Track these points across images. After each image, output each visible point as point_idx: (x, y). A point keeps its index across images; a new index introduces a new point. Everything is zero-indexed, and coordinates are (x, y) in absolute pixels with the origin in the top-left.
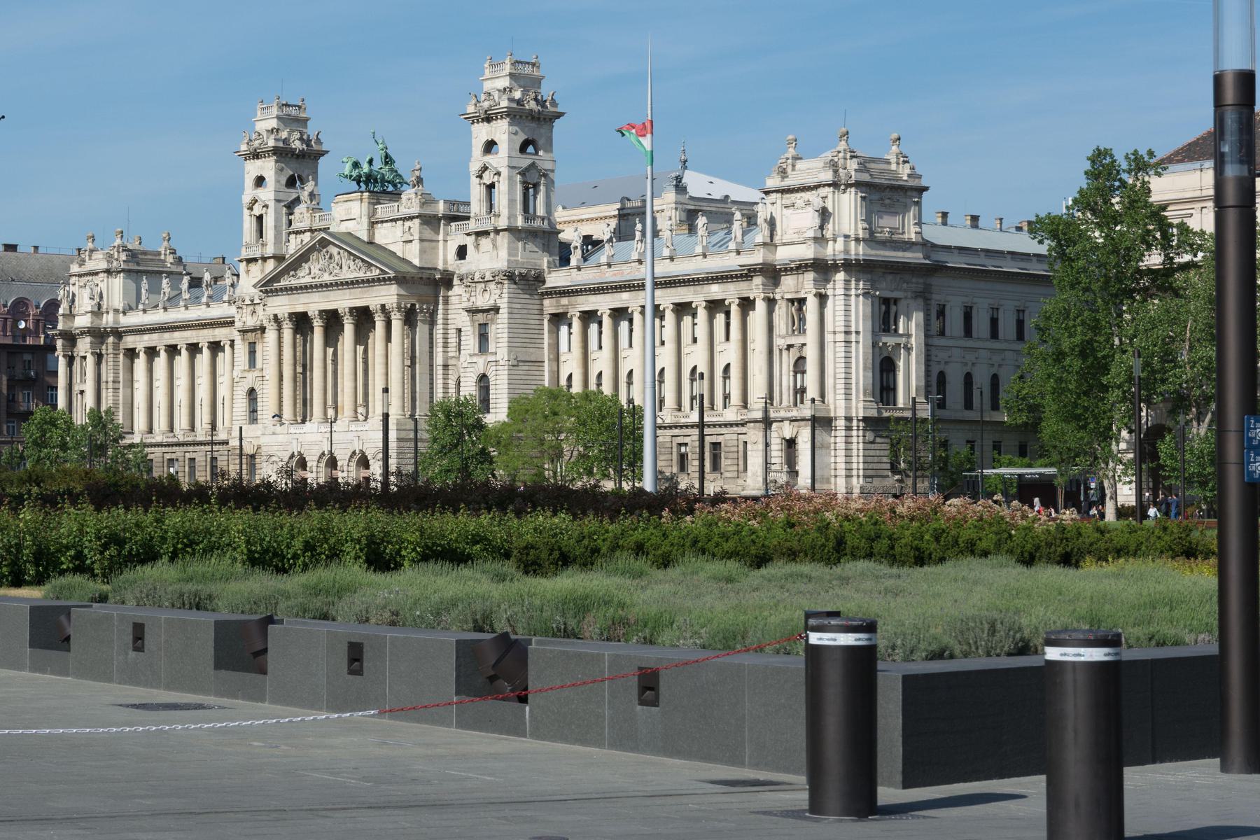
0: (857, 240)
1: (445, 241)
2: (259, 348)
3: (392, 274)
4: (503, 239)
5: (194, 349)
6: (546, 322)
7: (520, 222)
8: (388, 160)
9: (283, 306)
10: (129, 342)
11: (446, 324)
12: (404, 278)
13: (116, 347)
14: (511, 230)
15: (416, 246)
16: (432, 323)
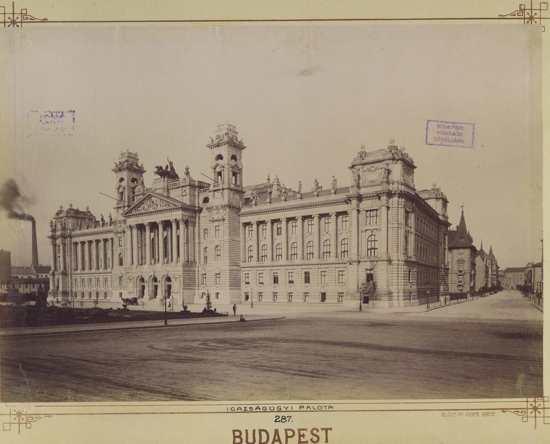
0: (402, 184)
1: (198, 196)
2: (123, 239)
3: (180, 206)
4: (226, 192)
5: (98, 241)
6: (241, 226)
7: (232, 186)
8: (172, 169)
9: (132, 221)
10: (75, 240)
11: (199, 227)
12: (184, 208)
13: (71, 241)
14: (229, 189)
15: (188, 197)
16: (194, 226)
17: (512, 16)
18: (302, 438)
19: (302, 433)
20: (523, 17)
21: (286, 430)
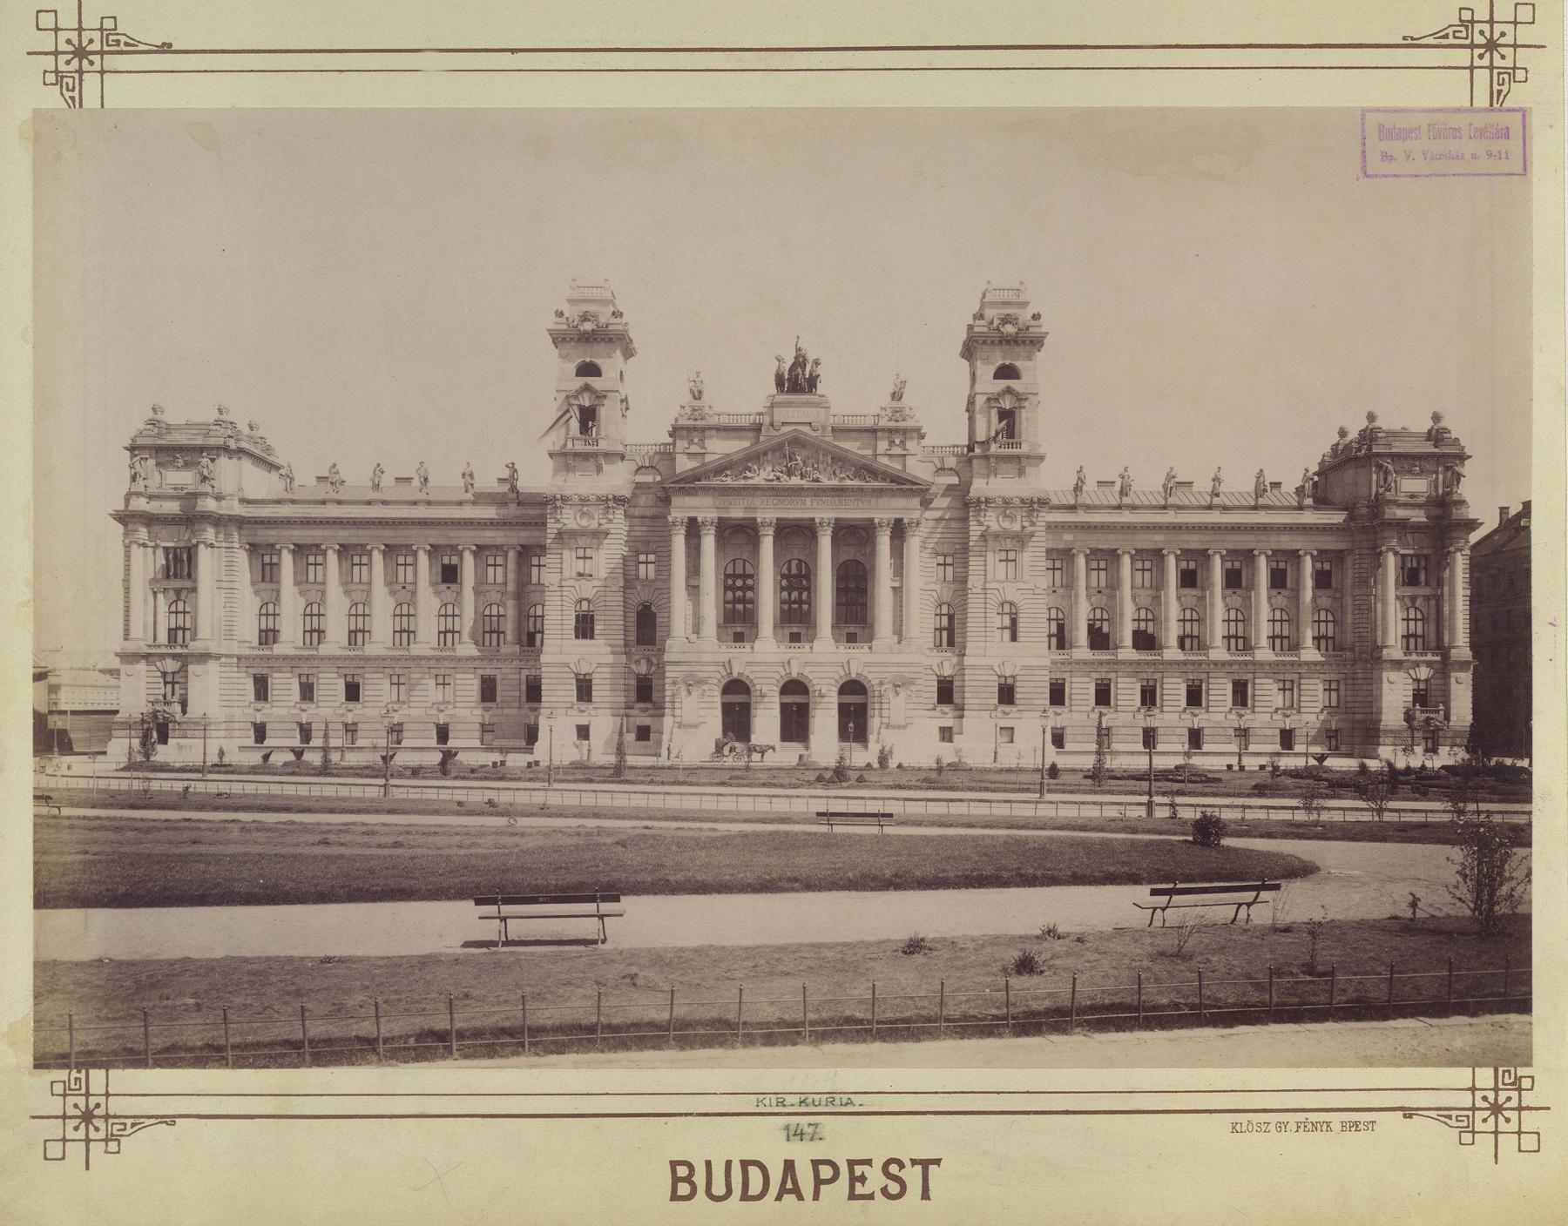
17: (1441, 40)
18: (858, 1185)
19: (858, 1170)
20: (1468, 42)
21: (816, 1164)
